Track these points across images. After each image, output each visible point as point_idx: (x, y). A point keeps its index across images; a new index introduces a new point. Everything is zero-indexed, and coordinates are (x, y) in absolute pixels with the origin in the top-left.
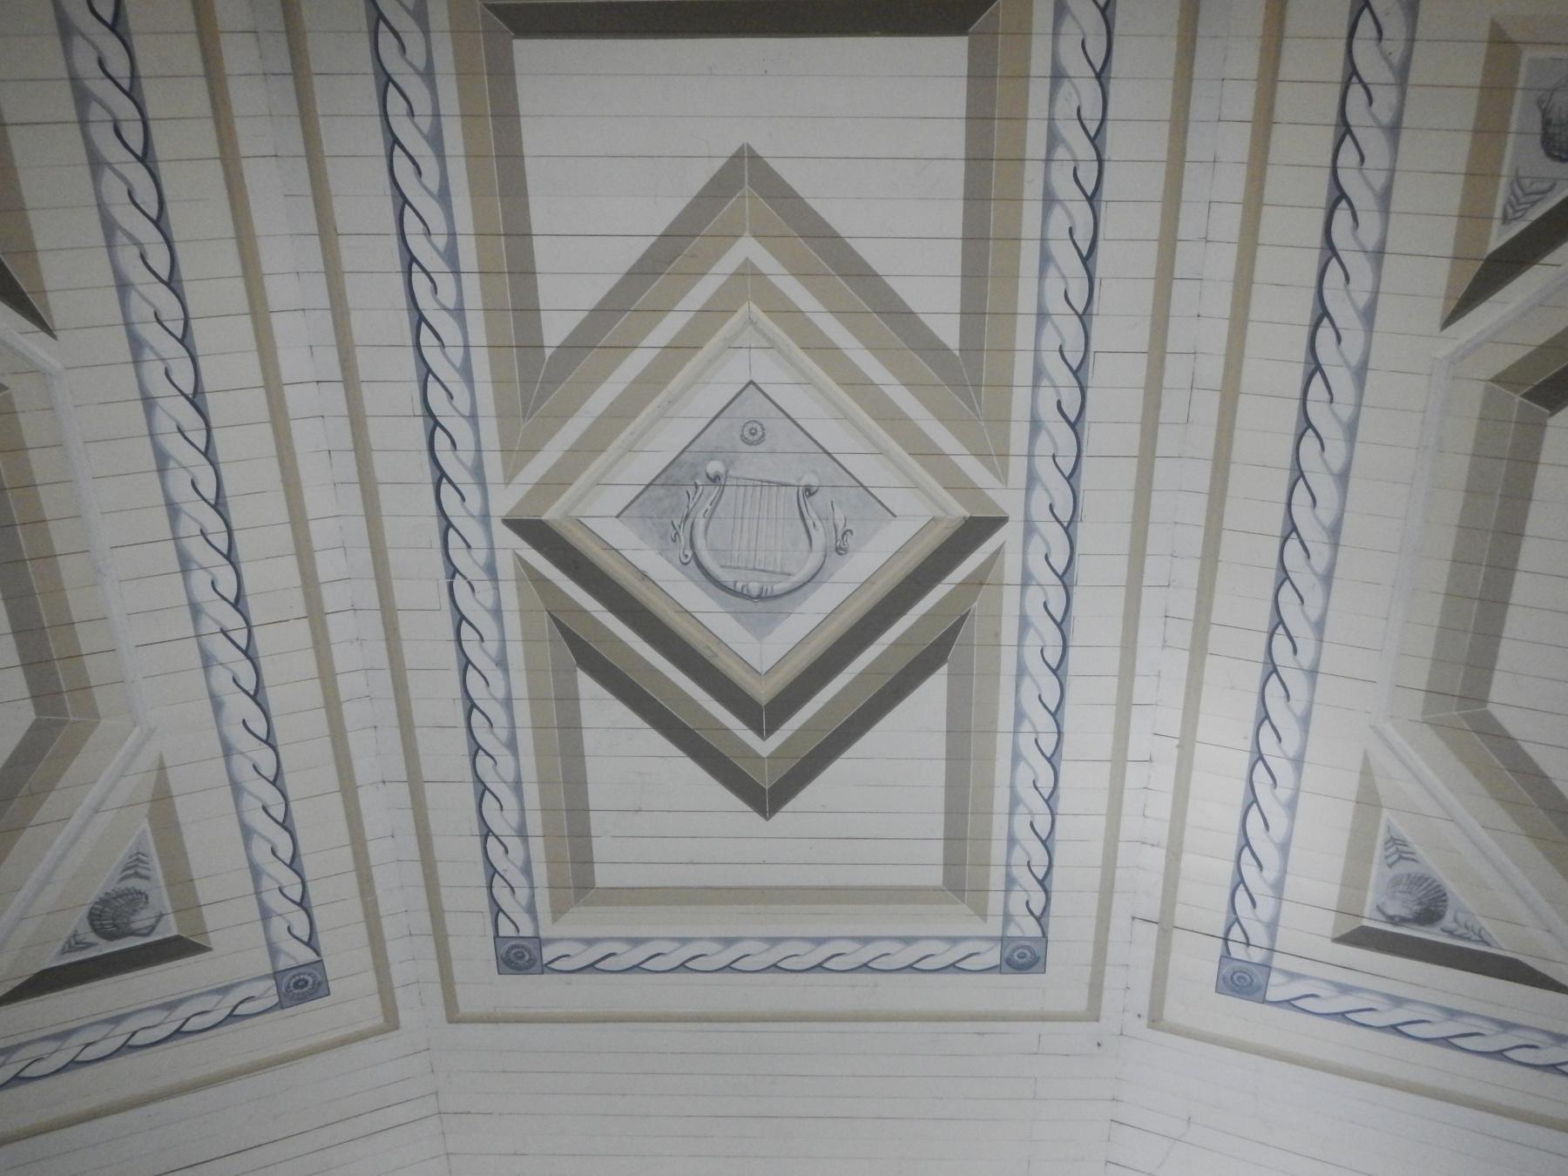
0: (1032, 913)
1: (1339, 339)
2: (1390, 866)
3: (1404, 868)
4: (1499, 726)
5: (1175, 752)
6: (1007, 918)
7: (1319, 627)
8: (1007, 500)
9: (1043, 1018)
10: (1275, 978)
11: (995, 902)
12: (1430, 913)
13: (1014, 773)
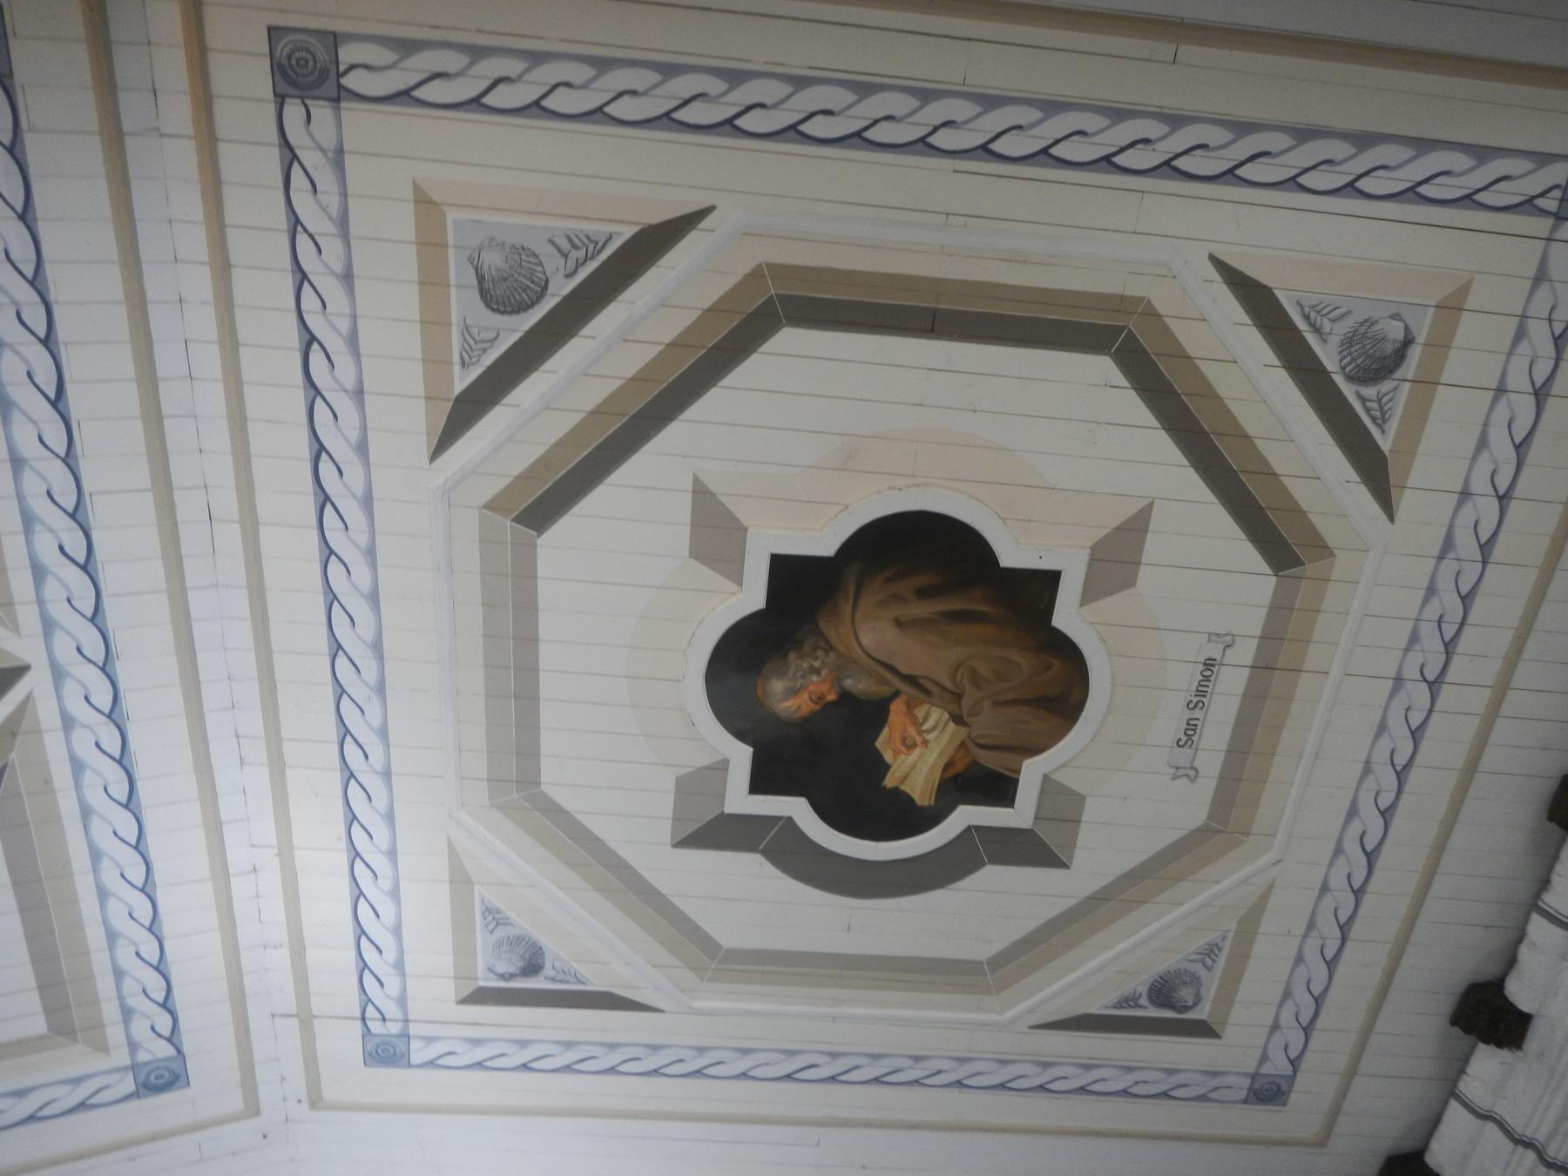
0: (160, 1035)
1: (341, 473)
2: (491, 932)
3: (501, 932)
4: (553, 803)
5: (277, 860)
6: (133, 1046)
7: (383, 732)
8: (25, 646)
9: (198, 1127)
10: (414, 1045)
11: (115, 1034)
12: (532, 967)
13: (102, 911)
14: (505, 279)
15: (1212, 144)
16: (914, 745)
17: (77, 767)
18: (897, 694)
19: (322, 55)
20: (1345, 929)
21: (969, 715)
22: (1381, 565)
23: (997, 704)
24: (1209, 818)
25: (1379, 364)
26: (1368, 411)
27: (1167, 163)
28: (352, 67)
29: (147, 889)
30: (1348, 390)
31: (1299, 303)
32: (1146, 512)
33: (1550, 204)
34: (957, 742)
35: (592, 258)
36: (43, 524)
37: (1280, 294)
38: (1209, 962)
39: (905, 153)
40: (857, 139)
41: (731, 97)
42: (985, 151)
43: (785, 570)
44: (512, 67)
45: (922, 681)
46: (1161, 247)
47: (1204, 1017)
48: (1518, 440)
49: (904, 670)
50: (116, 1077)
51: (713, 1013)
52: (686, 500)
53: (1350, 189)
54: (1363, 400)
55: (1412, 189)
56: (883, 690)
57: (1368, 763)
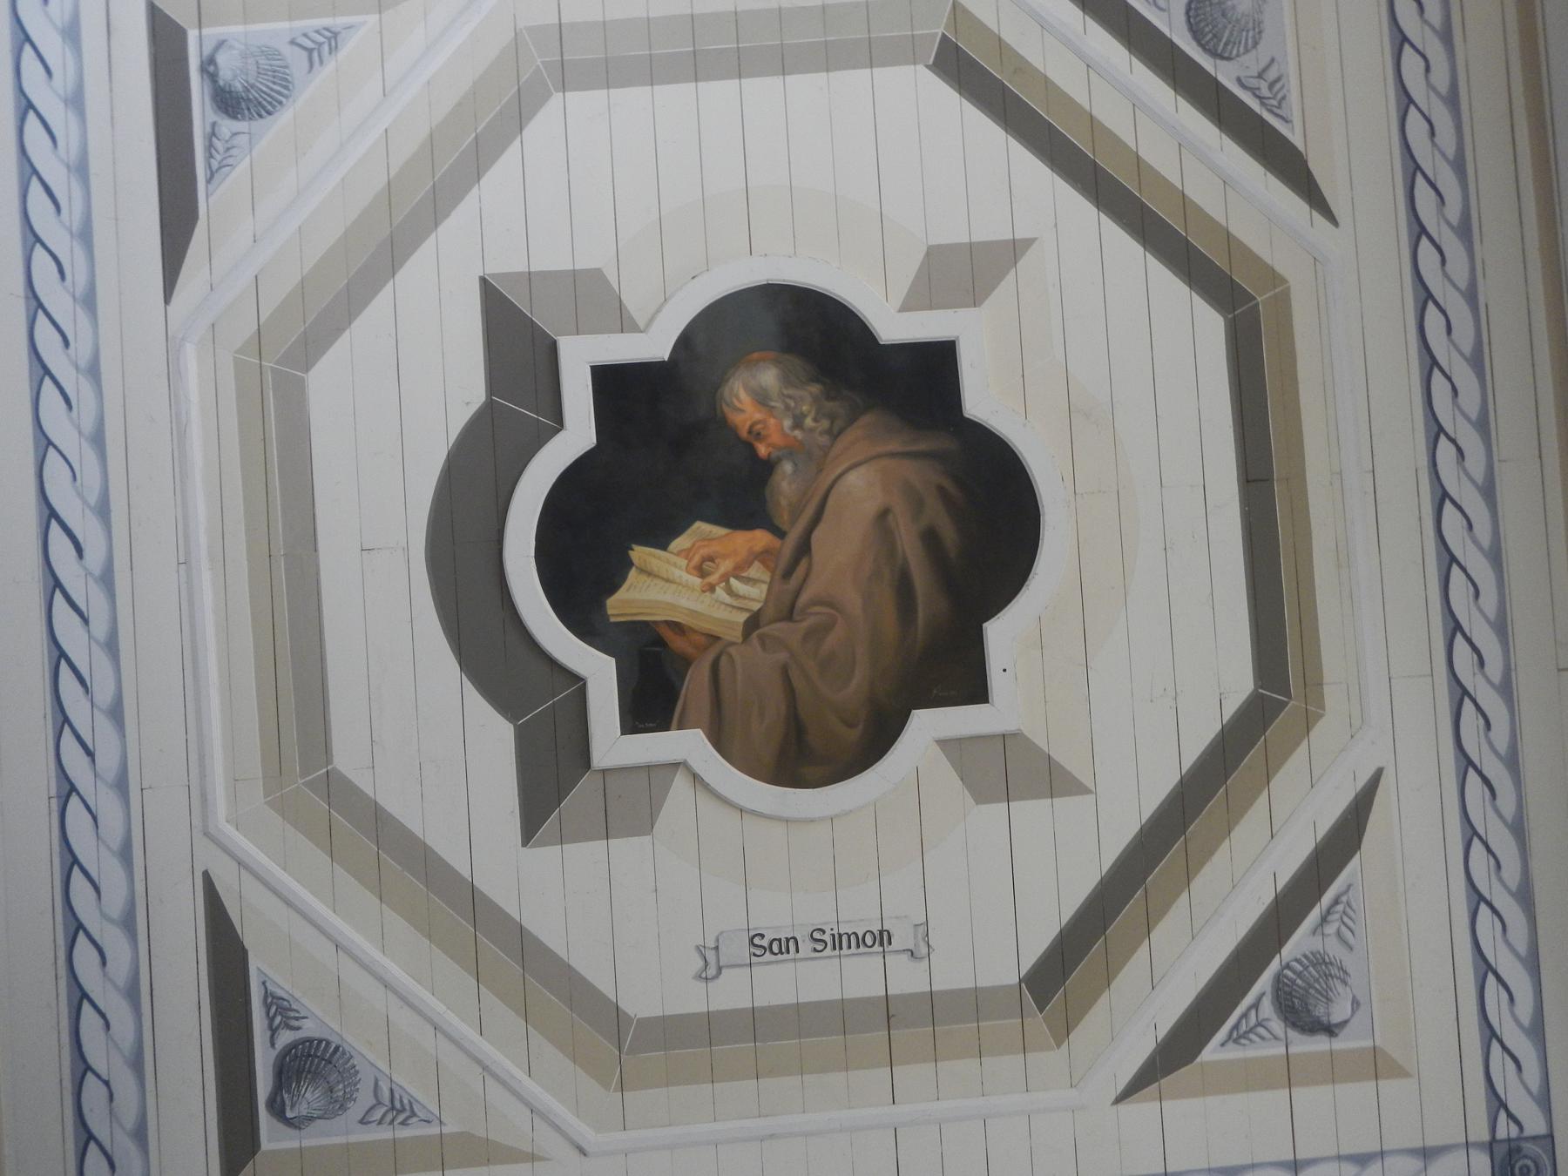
2: (293, 42)
14: (1224, 15)
15: (1492, 734)
16: (701, 572)
18: (780, 534)
21: (762, 639)
23: (785, 671)
25: (1299, 1012)
26: (1245, 1015)
27: (1465, 692)
31: (1349, 887)
32: (1075, 787)
33: (1504, 1129)
35: (1263, 104)
37: (1354, 863)
38: (378, 1114)
39: (1425, 416)
40: (1430, 363)
42: (1442, 497)
45: (804, 563)
47: (266, 1144)
49: (817, 535)
51: (173, 373)
53: (1477, 898)
54: (1256, 1005)
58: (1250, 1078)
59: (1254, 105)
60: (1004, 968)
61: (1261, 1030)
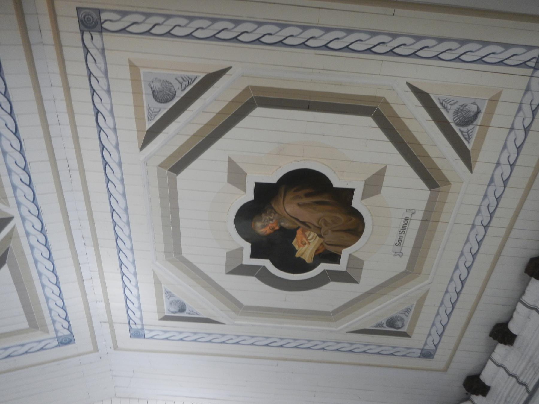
0: (65, 328)
1: (111, 155)
4: (186, 259)
5: (98, 276)
6: (56, 331)
7: (130, 237)
8: (12, 211)
9: (79, 355)
11: (51, 327)
14: (161, 92)
16: (305, 244)
17: (32, 248)
18: (299, 228)
19: (95, 16)
20: (453, 305)
21: (324, 235)
22: (467, 189)
23: (333, 231)
24: (407, 268)
25: (468, 119)
26: (463, 136)
27: (391, 51)
28: (105, 21)
29: (57, 284)
30: (456, 129)
31: (439, 99)
34: (320, 242)
35: (191, 84)
36: (15, 172)
37: (432, 96)
38: (407, 314)
39: (299, 48)
40: (280, 43)
41: (236, 30)
42: (326, 47)
43: (260, 187)
44: (160, 20)
46: (390, 80)
48: (518, 146)
49: (301, 219)
50: (52, 341)
51: (241, 325)
52: (226, 164)
53: (458, 59)
54: (462, 132)
55: (481, 59)
56: (294, 226)
57: (462, 252)
58: (481, 137)
59: (190, 87)
60: (424, 193)
61: (469, 132)
